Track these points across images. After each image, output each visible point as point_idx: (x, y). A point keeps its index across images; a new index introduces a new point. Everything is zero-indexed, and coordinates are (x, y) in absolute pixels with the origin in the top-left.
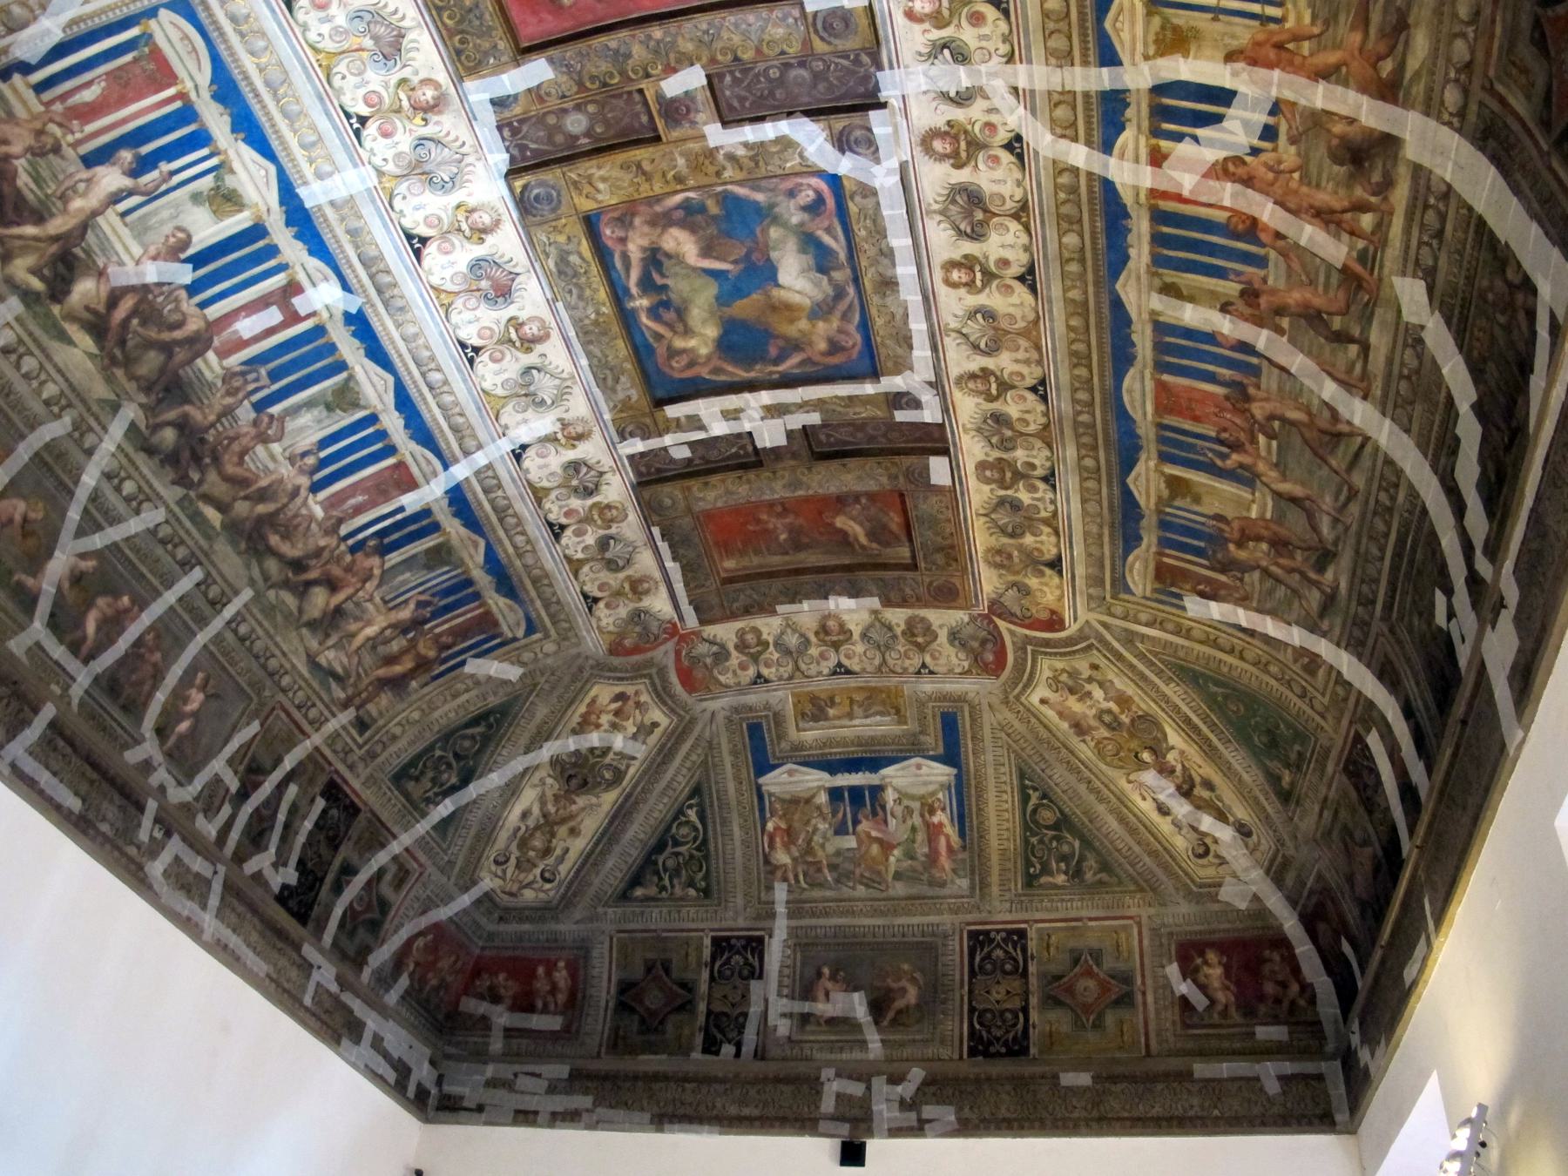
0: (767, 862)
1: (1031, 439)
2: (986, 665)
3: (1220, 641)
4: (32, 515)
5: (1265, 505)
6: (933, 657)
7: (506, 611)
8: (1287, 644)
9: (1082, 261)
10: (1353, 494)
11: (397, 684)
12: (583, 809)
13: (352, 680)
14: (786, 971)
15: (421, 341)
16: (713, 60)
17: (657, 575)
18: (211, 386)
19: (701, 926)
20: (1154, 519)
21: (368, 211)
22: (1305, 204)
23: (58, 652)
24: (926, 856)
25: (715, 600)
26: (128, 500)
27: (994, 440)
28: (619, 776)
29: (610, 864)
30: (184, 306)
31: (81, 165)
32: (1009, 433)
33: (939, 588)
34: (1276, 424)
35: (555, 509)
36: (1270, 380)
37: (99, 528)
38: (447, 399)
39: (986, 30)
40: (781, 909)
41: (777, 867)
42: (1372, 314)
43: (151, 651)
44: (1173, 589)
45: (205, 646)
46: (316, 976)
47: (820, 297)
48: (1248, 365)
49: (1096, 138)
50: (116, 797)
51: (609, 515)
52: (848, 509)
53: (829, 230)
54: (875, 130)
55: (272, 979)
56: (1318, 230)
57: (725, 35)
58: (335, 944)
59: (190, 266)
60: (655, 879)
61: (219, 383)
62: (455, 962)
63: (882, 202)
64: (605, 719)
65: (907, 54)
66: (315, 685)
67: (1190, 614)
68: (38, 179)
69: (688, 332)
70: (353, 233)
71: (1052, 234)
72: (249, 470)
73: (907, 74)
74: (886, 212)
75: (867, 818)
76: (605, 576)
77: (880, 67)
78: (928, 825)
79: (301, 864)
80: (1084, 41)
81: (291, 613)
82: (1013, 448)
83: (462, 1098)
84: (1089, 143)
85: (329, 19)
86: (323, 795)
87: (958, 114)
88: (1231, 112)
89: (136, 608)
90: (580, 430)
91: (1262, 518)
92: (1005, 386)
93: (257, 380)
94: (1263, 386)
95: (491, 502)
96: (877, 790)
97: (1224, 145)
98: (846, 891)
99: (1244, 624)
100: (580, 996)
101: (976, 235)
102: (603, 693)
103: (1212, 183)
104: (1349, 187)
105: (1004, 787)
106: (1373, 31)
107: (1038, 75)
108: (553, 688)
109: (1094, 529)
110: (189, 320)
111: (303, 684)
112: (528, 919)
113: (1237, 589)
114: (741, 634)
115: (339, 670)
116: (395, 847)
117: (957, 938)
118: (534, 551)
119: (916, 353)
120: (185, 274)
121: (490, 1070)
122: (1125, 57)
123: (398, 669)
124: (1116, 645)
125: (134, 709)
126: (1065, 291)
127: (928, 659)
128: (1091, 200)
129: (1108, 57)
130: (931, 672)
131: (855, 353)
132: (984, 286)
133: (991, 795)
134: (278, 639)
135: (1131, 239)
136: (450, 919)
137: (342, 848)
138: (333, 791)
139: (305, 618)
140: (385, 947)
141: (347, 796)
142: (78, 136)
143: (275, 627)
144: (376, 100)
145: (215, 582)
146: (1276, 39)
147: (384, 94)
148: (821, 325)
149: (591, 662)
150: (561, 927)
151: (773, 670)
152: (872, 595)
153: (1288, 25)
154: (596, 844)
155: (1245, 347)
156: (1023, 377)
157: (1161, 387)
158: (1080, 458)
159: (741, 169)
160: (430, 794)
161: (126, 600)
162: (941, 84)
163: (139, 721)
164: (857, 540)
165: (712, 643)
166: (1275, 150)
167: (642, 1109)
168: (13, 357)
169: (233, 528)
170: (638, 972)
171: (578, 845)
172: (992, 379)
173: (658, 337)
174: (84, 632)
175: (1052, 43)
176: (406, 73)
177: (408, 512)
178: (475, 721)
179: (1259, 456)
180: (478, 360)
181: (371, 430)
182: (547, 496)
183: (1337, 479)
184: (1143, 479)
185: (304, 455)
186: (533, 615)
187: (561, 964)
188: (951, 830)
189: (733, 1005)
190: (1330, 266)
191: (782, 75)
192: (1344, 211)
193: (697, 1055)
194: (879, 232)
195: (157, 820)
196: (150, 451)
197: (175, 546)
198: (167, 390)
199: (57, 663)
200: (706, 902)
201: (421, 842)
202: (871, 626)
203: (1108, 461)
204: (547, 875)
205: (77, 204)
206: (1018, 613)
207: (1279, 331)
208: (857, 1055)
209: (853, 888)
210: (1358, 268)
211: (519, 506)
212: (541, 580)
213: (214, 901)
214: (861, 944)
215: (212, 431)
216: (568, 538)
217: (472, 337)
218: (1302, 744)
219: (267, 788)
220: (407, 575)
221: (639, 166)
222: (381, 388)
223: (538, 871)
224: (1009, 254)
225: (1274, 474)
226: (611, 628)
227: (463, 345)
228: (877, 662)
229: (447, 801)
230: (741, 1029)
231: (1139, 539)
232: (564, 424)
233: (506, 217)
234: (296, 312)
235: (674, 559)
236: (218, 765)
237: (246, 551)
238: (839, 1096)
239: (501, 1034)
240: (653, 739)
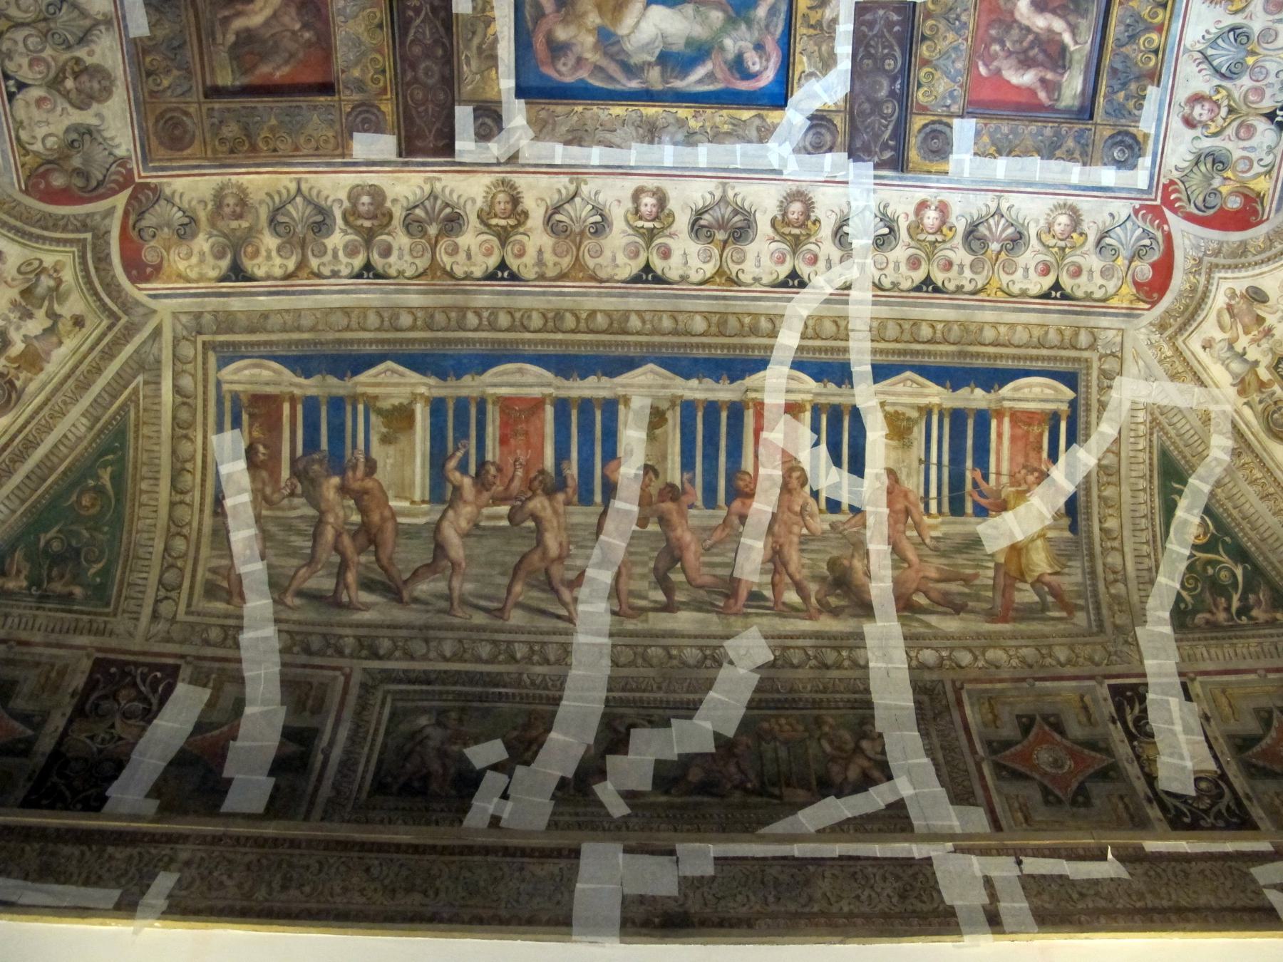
1: (428, 255)
2: (44, 175)
3: (188, 477)
5: (415, 516)
6: (40, 102)
8: (231, 557)
9: (675, 332)
10: (499, 613)
16: (929, 15)
20: (342, 392)
22: (782, 540)
27: (418, 212)
32: (433, 230)
33: (177, 124)
34: (531, 524)
36: (582, 516)
39: (903, 268)
42: (708, 611)
44: (245, 417)
47: (628, 47)
48: (591, 492)
49: (807, 356)
52: (293, 11)
53: (711, 76)
54: (829, 156)
56: (762, 552)
57: (951, 36)
63: (749, 146)
65: (887, 194)
67: (214, 439)
71: (703, 305)
73: (868, 191)
74: (739, 147)
77: (877, 167)
80: (894, 352)
82: (409, 233)
84: (800, 349)
87: (826, 231)
88: (845, 473)
91: (394, 514)
92: (504, 236)
94: (571, 508)
97: (815, 467)
99: (229, 503)
101: (697, 228)
103: (779, 457)
104: (814, 578)
106: (942, 586)
107: (861, 310)
109: (307, 321)
113: (277, 489)
119: (559, 148)
122: (882, 386)
124: (129, 349)
126: (638, 312)
127: (35, 93)
128: (742, 347)
129: (881, 372)
131: (548, 71)
132: (635, 229)
135: (708, 382)
146: (913, 510)
148: (590, 40)
152: (152, 26)
153: (925, 518)
155: (610, 489)
156: (521, 254)
157: (538, 404)
158: (410, 310)
159: (809, 8)
162: (856, 219)
164: (239, 14)
166: (821, 511)
172: (512, 222)
175: (891, 324)
179: (480, 508)
183: (503, 593)
184: (396, 379)
190: (732, 565)
191: (886, 71)
192: (791, 577)
194: (717, 137)
202: (84, 14)
203: (413, 341)
206: (144, 223)
207: (643, 522)
210: (743, 594)
218: (86, 597)
224: (676, 259)
225: (464, 524)
231: (308, 375)
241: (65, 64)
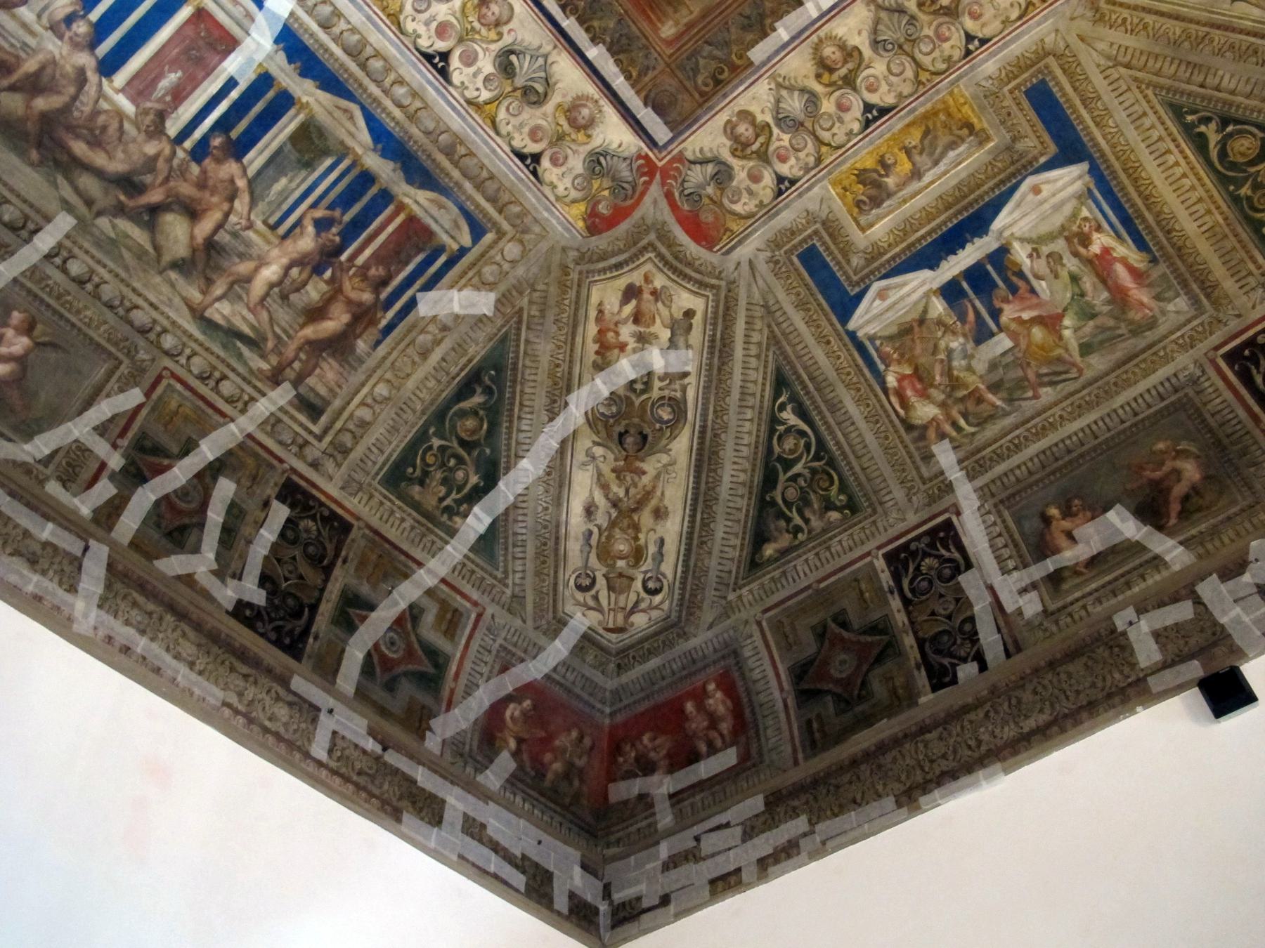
0: (909, 427)
6: (975, 17)
7: (434, 210)
12: (657, 477)
13: (270, 344)
14: (1000, 542)
17: (590, 89)
19: (866, 549)
24: (1109, 302)
25: (670, 83)
28: (678, 407)
29: (720, 534)
35: (422, 30)
40: (955, 475)
41: (925, 428)
45: (15, 280)
46: (326, 725)
51: (491, 18)
55: (237, 712)
60: (782, 523)
62: (581, 738)
64: (627, 332)
66: (222, 354)
75: (1006, 301)
76: (533, 117)
78: (1089, 262)
79: (265, 580)
81: (146, 252)
83: (639, 899)
86: (282, 498)
96: (1000, 256)
98: (1028, 407)
100: (747, 712)
105: (1162, 146)
108: (543, 312)
111: (198, 348)
112: (651, 653)
115: (246, 330)
116: (425, 578)
117: (1211, 372)
121: (664, 850)
123: (330, 326)
127: (969, 24)
130: (983, 42)
133: (1151, 168)
134: (137, 285)
136: (547, 677)
137: (338, 571)
138: (293, 493)
139: (167, 258)
140: (456, 711)
141: (322, 504)
143: (126, 268)
149: (573, 254)
150: (694, 642)
151: (792, 161)
154: (693, 516)
160: (448, 502)
165: (704, 162)
167: (879, 796)
170: (809, 647)
171: (672, 528)
178: (465, 390)
186: (470, 207)
187: (711, 687)
188: (1125, 250)
189: (949, 617)
193: (926, 698)
200: (860, 516)
201: (459, 569)
202: (877, 22)
204: (651, 585)
208: (1154, 579)
209: (1036, 397)
211: (375, 38)
214: (1082, 456)
219: (179, 474)
220: (283, 181)
223: (638, 585)
226: (574, 194)
228: (909, 73)
229: (476, 509)
230: (973, 637)
235: (594, 40)
236: (79, 429)
237: (41, 163)
238: (1156, 635)
239: (667, 804)
240: (696, 336)
241: (930, 13)
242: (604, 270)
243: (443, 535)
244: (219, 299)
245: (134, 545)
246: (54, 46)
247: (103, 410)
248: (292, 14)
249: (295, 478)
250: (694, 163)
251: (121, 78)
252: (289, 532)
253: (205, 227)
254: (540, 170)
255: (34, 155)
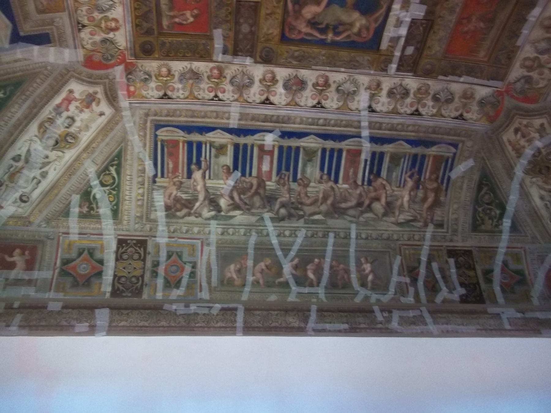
4: (267, 263)
11: (437, 203)
13: (419, 217)
15: (304, 119)
17: (467, 86)
18: (277, 189)
21: (248, 111)
23: (306, 290)
26: (290, 236)
30: (247, 180)
31: (189, 180)
35: (406, 109)
37: (290, 250)
38: (332, 122)
43: (338, 267)
45: (356, 251)
46: (504, 317)
50: (359, 314)
58: (505, 298)
59: (236, 171)
61: (279, 186)
68: (186, 193)
69: (352, 25)
70: (253, 119)
72: (313, 197)
76: (452, 106)
79: (462, 285)
85: (178, 90)
86: (449, 257)
89: (322, 260)
90: (375, 84)
93: (285, 175)
95: (385, 130)
102: (508, 136)
110: (252, 181)
114: (523, 66)
118: (419, 126)
120: (238, 174)
123: (430, 200)
125: (347, 285)
134: (379, 228)
138: (452, 253)
139: (380, 215)
141: (460, 250)
142: (181, 175)
144: (211, 89)
145: (339, 232)
147: (210, 85)
161: (316, 260)
163: (351, 287)
165: (519, 80)
168: (226, 233)
169: (327, 214)
173: (348, 36)
174: (309, 278)
176: (206, 75)
177: (369, 159)
178: (479, 189)
180: (323, 104)
181: (328, 153)
182: (397, 109)
185: (321, 178)
186: (450, 141)
195: (382, 311)
196: (282, 219)
197: (317, 234)
198: (269, 202)
199: (308, 293)
201: (510, 240)
205: (199, 188)
211: (395, 121)
212: (435, 130)
213: (429, 319)
215: (292, 199)
216: (423, 111)
217: (312, 102)
219: (422, 270)
220: (394, 174)
221: (267, 14)
222: (315, 141)
226: (479, 116)
227: (314, 107)
229: (504, 220)
232: (368, 88)
233: (271, 68)
234: (270, 151)
235: (460, 76)
236: (395, 279)
242: (503, 130)
243: (498, 234)
244: (399, 216)
245: (428, 301)
246: (322, 187)
247: (396, 268)
248: (370, 133)
249: (449, 248)
250: (515, 82)
251: (341, 181)
252: (458, 266)
253: (383, 200)
254: (465, 118)
255: (336, 216)
